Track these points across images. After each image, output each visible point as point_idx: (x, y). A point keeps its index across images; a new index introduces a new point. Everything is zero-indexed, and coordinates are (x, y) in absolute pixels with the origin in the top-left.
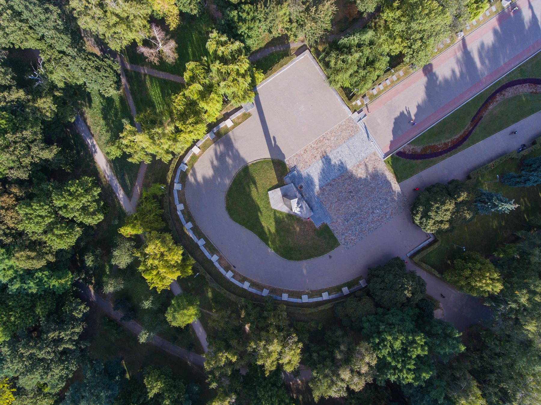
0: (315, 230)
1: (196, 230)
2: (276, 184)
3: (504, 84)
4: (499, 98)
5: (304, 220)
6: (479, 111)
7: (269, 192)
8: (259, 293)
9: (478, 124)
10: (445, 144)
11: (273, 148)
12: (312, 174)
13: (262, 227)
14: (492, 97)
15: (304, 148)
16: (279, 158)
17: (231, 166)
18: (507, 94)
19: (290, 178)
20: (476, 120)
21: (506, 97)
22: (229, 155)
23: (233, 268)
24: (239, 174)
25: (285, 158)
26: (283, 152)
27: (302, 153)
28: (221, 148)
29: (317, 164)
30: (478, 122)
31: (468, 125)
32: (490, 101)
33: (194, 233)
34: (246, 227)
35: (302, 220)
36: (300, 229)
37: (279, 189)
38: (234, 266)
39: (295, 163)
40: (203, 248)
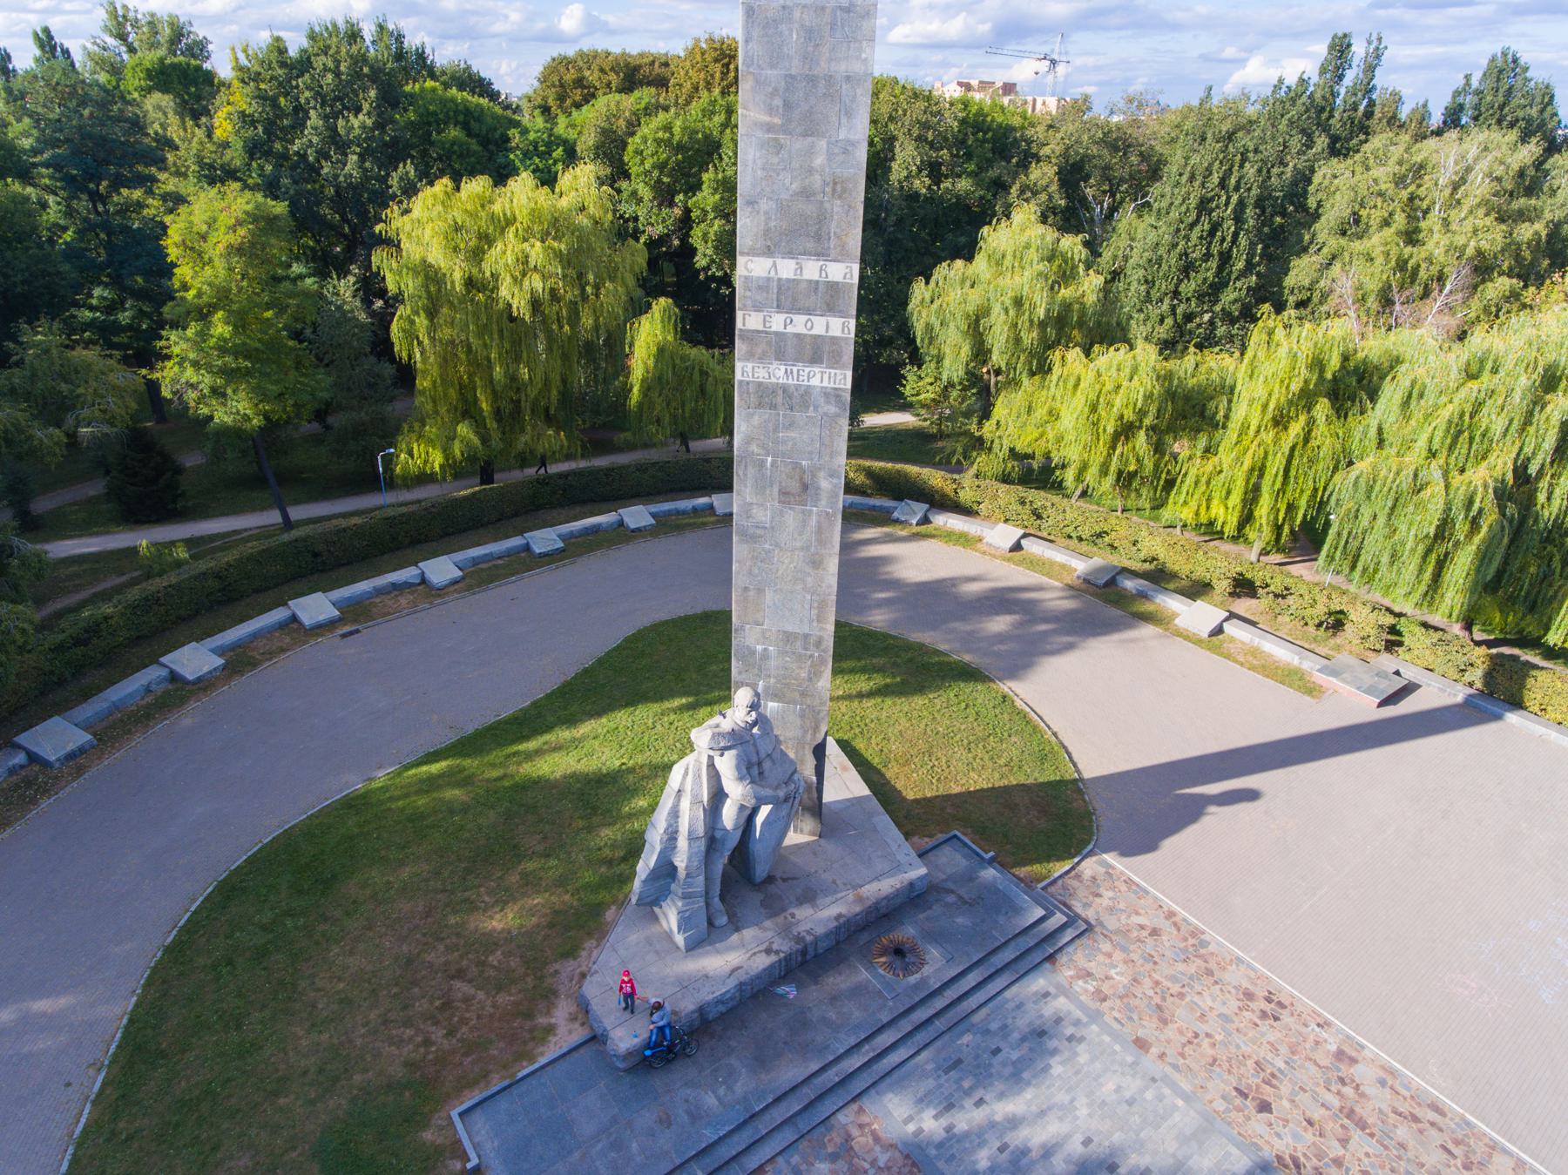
0: (425, 1089)
1: (621, 535)
2: (899, 786)
5: (569, 967)
11: (1163, 801)
12: (1057, 1068)
13: (572, 721)
15: (1286, 989)
16: (1106, 817)
17: (958, 625)
19: (970, 877)
22: (1021, 624)
23: (347, 629)
24: (921, 648)
25: (1127, 852)
26: (1170, 844)
27: (1234, 976)
28: (1055, 599)
29: (1184, 1118)
33: (596, 529)
34: (586, 671)
35: (571, 953)
36: (490, 942)
37: (862, 789)
38: (357, 631)
39: (1111, 923)
40: (515, 542)
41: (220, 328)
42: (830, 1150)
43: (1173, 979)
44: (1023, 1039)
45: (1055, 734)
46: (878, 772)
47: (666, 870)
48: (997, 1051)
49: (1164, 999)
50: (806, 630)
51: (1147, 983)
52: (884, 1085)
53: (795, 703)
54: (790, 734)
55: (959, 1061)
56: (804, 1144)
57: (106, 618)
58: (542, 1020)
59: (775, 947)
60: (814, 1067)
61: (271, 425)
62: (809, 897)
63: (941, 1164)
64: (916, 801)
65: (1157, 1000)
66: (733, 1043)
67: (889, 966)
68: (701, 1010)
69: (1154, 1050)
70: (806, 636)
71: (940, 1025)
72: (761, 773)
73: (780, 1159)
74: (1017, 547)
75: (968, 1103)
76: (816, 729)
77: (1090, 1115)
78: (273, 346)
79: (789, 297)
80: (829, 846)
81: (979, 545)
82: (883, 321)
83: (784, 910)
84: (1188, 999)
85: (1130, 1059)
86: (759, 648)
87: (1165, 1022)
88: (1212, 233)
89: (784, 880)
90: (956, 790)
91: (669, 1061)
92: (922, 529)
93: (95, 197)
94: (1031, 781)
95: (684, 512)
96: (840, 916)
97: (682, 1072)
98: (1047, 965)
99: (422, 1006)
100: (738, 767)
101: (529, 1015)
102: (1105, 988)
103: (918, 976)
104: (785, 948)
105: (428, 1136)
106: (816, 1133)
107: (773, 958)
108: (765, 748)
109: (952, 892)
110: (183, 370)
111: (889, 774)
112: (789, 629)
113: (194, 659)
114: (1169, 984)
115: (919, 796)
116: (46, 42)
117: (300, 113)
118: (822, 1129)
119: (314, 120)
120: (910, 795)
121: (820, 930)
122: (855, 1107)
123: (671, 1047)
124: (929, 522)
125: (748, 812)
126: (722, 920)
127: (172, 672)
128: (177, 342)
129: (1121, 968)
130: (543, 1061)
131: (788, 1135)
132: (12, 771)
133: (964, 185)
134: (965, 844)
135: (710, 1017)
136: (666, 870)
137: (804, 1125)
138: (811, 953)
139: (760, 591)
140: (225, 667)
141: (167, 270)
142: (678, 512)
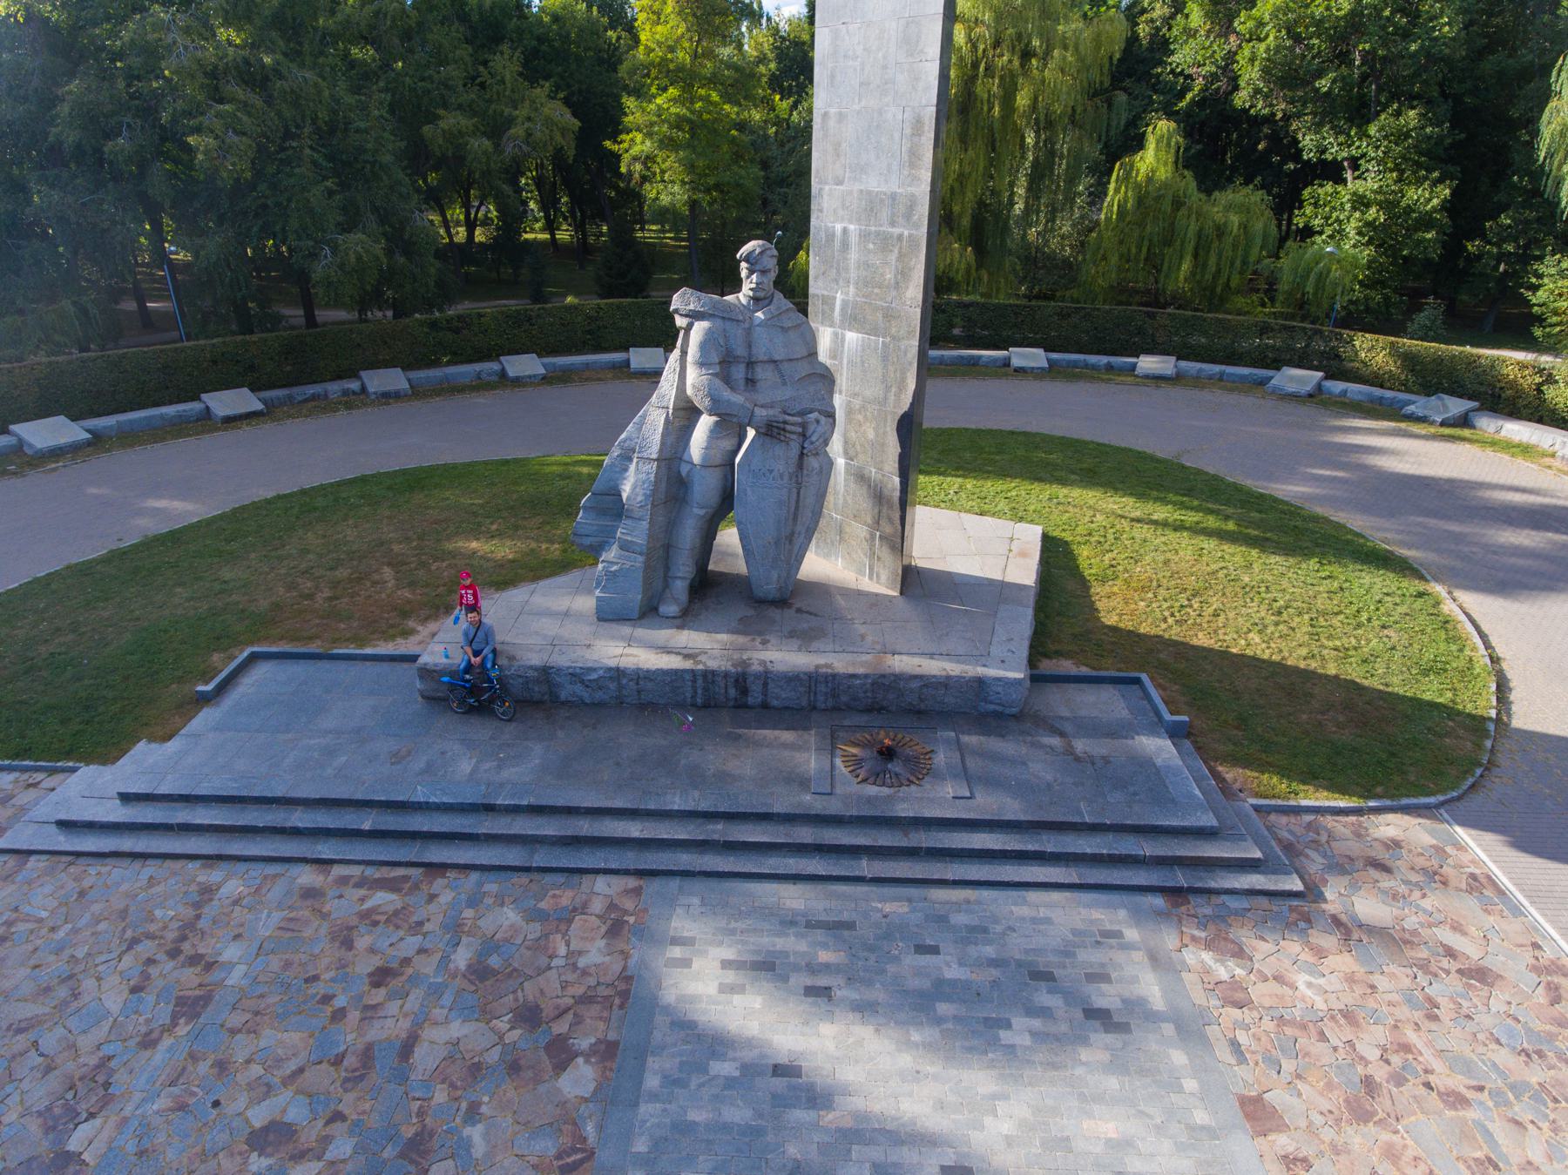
2: (1099, 605)
7: (1031, 535)
8: (421, 375)
33: (974, 363)
42: (543, 905)
43: (1459, 1064)
44: (994, 963)
45: (1495, 660)
46: (1084, 584)
48: (934, 950)
49: (1399, 1080)
50: (893, 186)
51: (1380, 1034)
52: (699, 885)
53: (874, 331)
54: (868, 393)
55: (850, 926)
56: (523, 879)
57: (480, 316)
58: (411, 624)
59: (703, 658)
60: (619, 803)
62: (806, 638)
63: (659, 1019)
64: (1114, 629)
65: (1380, 1073)
66: (560, 734)
67: (857, 763)
68: (546, 672)
69: (1283, 1142)
70: (893, 197)
71: (865, 867)
72: (751, 382)
73: (474, 876)
75: (801, 980)
76: (902, 387)
77: (1009, 1141)
80: (902, 603)
81: (1547, 461)
82: (1538, 220)
83: (760, 633)
84: (1471, 1114)
85: (1201, 1117)
86: (839, 227)
87: (1361, 1115)
89: (799, 611)
90: (1202, 640)
91: (471, 710)
92: (1447, 431)
94: (1374, 683)
95: (1094, 367)
96: (826, 666)
97: (481, 730)
98: (1158, 901)
99: (342, 573)
100: (704, 346)
101: (405, 615)
102: (1260, 992)
103: (886, 791)
104: (713, 664)
105: (216, 657)
106: (549, 878)
107: (688, 665)
108: (766, 344)
109: (1062, 734)
111: (1097, 589)
112: (873, 183)
113: (525, 365)
114: (1437, 1065)
115: (1127, 624)
118: (560, 878)
120: (1111, 620)
121: (779, 667)
122: (632, 882)
123: (483, 692)
124: (1473, 427)
125: (728, 444)
126: (670, 609)
127: (503, 369)
128: (634, 111)
129: (1333, 982)
130: (368, 651)
131: (513, 856)
132: (346, 393)
134: (1147, 696)
135: (563, 695)
137: (541, 858)
138: (755, 698)
139: (841, 117)
140: (544, 378)
142: (1086, 365)
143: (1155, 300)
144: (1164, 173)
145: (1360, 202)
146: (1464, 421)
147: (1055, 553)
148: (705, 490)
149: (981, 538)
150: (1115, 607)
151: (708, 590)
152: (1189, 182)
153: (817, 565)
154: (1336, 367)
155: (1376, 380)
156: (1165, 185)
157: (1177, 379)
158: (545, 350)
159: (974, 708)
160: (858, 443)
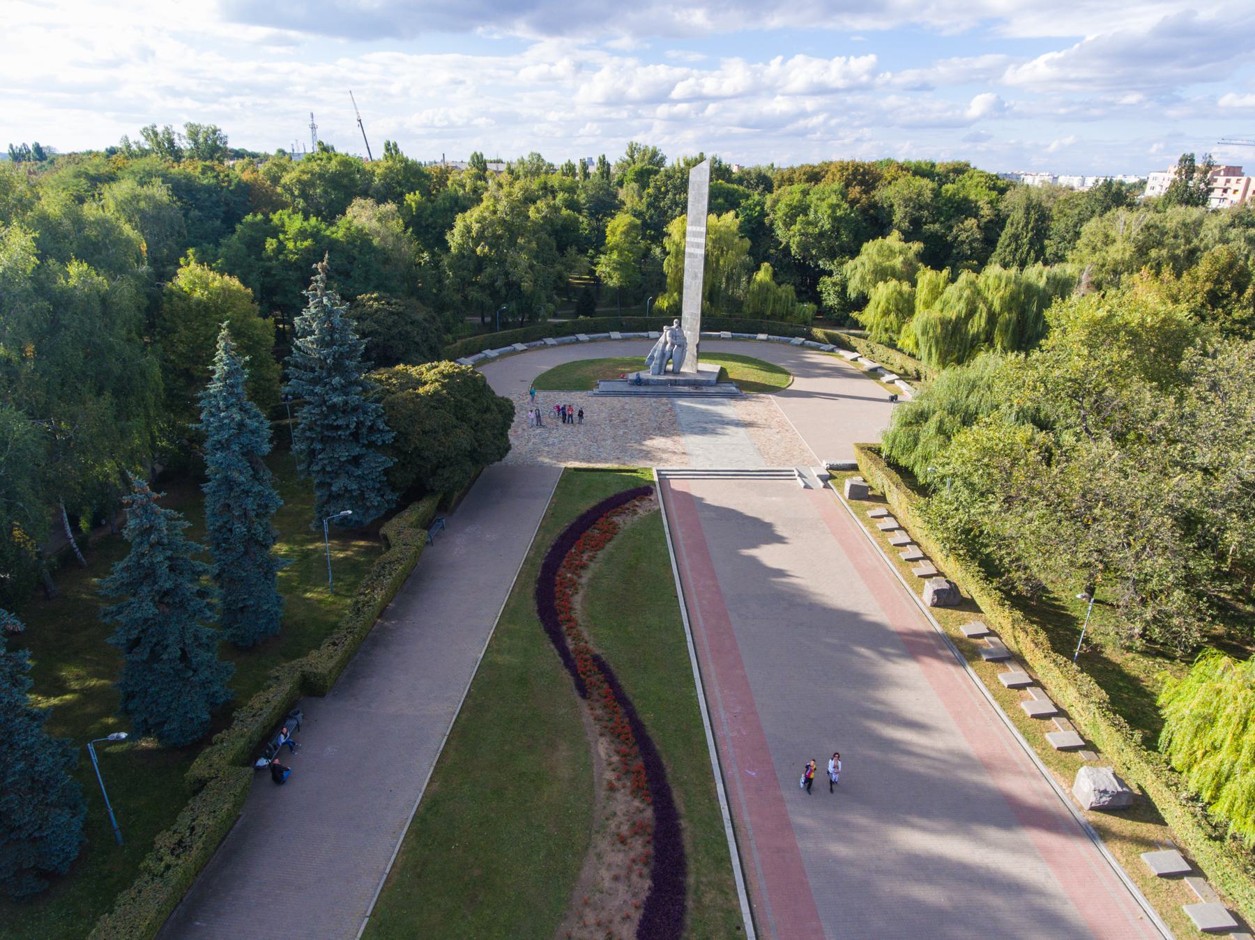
3: (691, 880)
4: (626, 807)
6: (619, 697)
9: (565, 674)
10: (584, 567)
14: (652, 779)
18: (619, 858)
20: (593, 676)
21: (603, 844)
30: (575, 673)
31: (591, 635)
32: (639, 762)
37: (717, 370)
41: (615, 256)
47: (652, 358)
61: (621, 287)
74: (856, 360)
78: (628, 264)
79: (695, 234)
88: (1016, 250)
93: (598, 220)
110: (601, 270)
113: (582, 337)
116: (603, 162)
117: (667, 192)
119: (670, 195)
133: (937, 226)
136: (652, 358)
141: (605, 237)
143: (763, 315)
144: (768, 278)
145: (834, 284)
146: (832, 351)
147: (723, 371)
148: (668, 355)
149: (712, 367)
150: (731, 376)
151: (666, 372)
152: (773, 283)
153: (682, 370)
154: (809, 337)
155: (819, 341)
156: (767, 283)
157: (768, 340)
158: (586, 333)
159: (708, 384)
160: (691, 350)
